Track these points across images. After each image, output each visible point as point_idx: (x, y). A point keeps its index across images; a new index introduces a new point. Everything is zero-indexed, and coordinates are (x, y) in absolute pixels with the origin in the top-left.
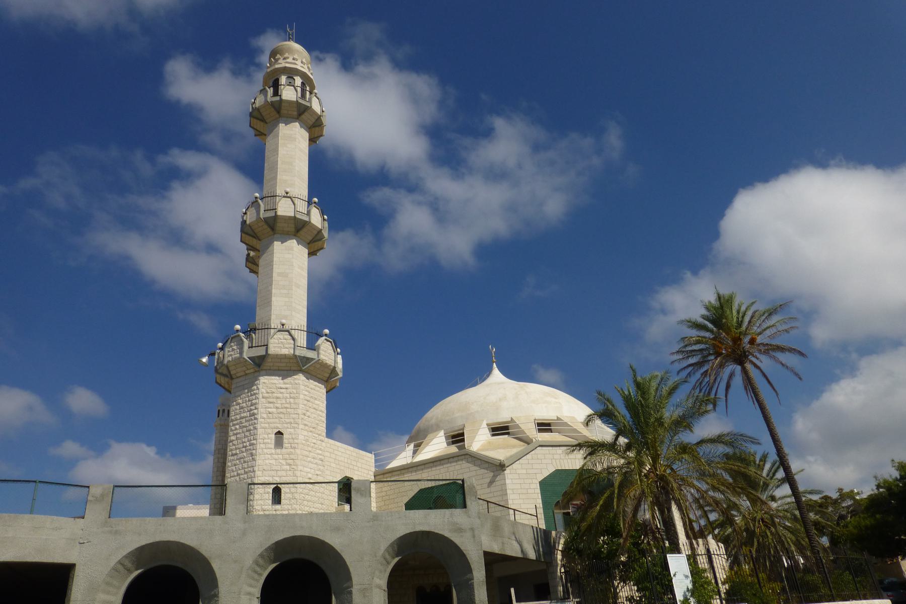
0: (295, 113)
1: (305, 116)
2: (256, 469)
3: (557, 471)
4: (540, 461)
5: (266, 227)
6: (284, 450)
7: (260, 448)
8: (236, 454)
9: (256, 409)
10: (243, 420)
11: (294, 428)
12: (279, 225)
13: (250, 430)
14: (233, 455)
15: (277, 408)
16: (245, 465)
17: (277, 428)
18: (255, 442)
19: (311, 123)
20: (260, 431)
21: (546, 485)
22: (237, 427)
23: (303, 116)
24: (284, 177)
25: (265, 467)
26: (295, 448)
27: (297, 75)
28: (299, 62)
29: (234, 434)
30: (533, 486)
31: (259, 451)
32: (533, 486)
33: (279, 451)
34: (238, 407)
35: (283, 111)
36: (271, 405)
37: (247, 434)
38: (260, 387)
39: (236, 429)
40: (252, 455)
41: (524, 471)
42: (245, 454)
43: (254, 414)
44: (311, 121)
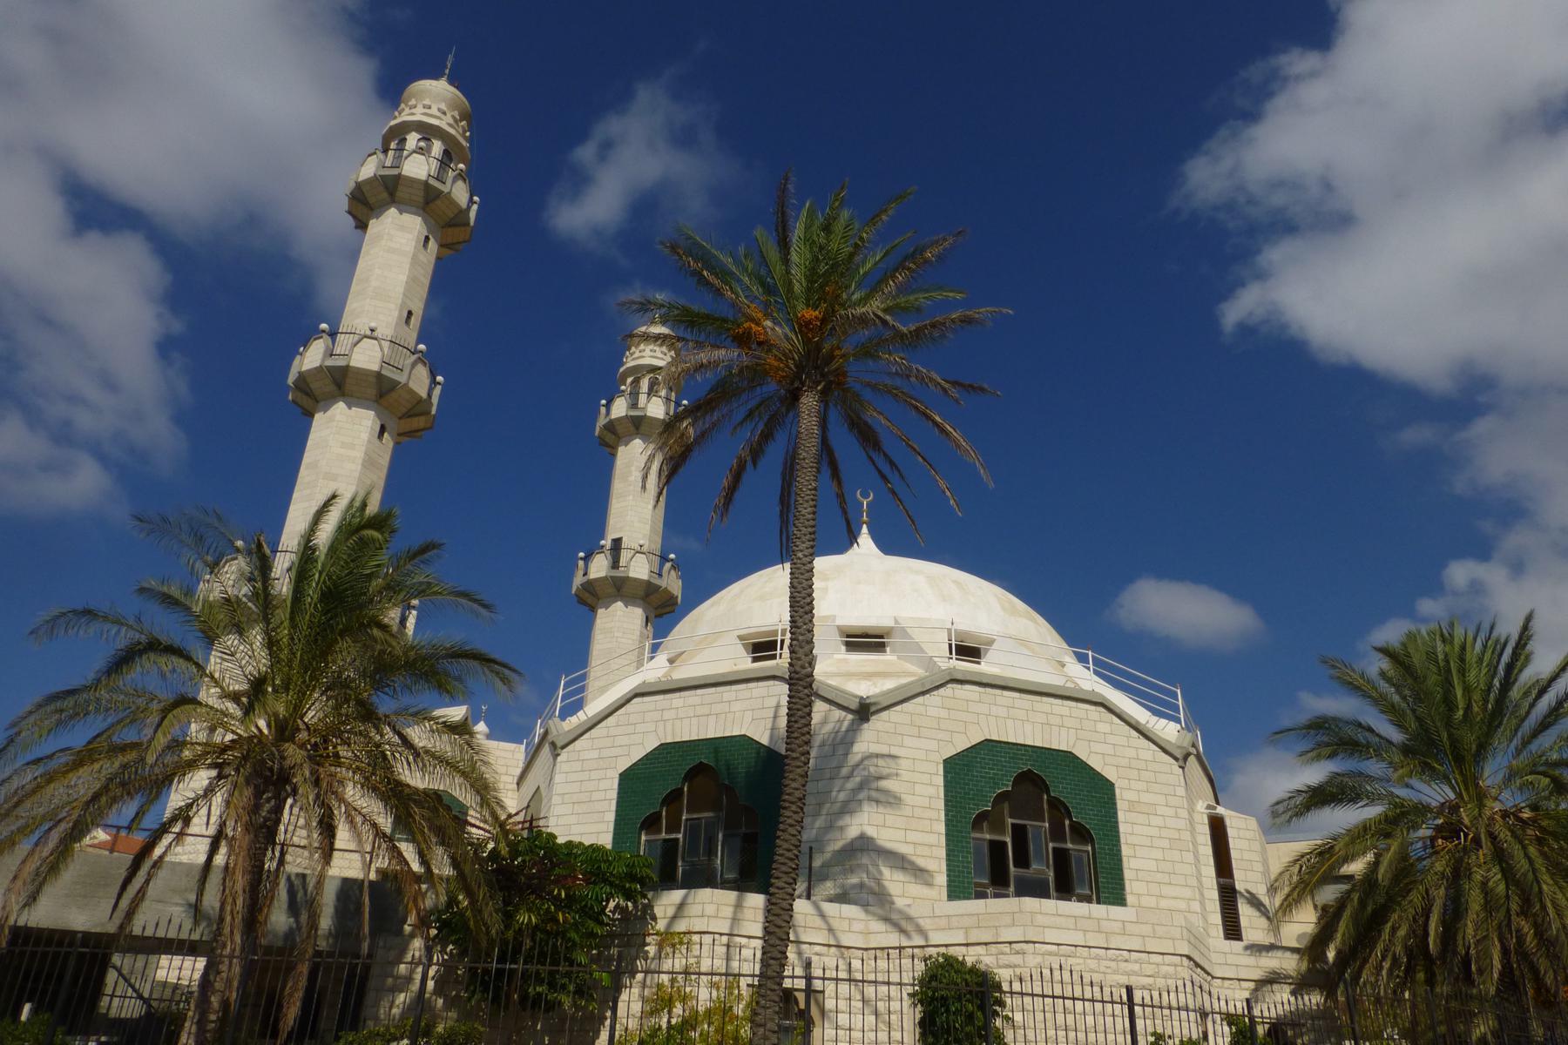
0: (385, 195)
1: (402, 193)
3: (988, 742)
4: (630, 729)
12: (314, 386)
19: (421, 200)
21: (631, 781)
23: (399, 194)
24: (355, 305)
27: (409, 132)
28: (420, 109)
30: (603, 785)
32: (603, 785)
35: (372, 200)
41: (595, 754)
44: (419, 196)
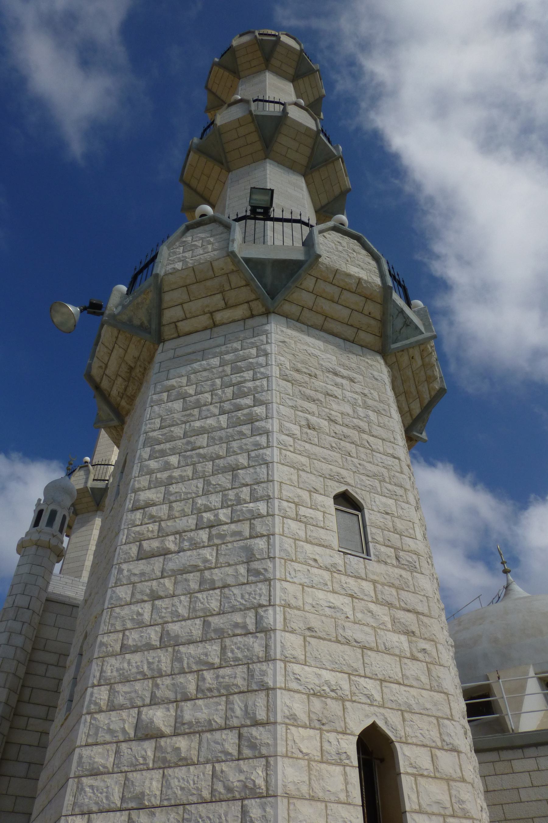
2: (274, 617)
5: (254, 137)
6: (375, 568)
7: (287, 531)
8: (165, 553)
9: (257, 402)
10: (203, 440)
11: (393, 496)
13: (234, 469)
14: (143, 556)
15: (331, 420)
16: (212, 601)
17: (341, 480)
18: (262, 507)
20: (280, 472)
22: (174, 460)
25: (315, 622)
26: (412, 568)
29: (154, 485)
31: (282, 545)
33: (356, 563)
34: (178, 405)
36: (312, 407)
37: (224, 480)
38: (273, 349)
39: (167, 467)
40: (250, 557)
42: (208, 554)
43: (251, 420)
